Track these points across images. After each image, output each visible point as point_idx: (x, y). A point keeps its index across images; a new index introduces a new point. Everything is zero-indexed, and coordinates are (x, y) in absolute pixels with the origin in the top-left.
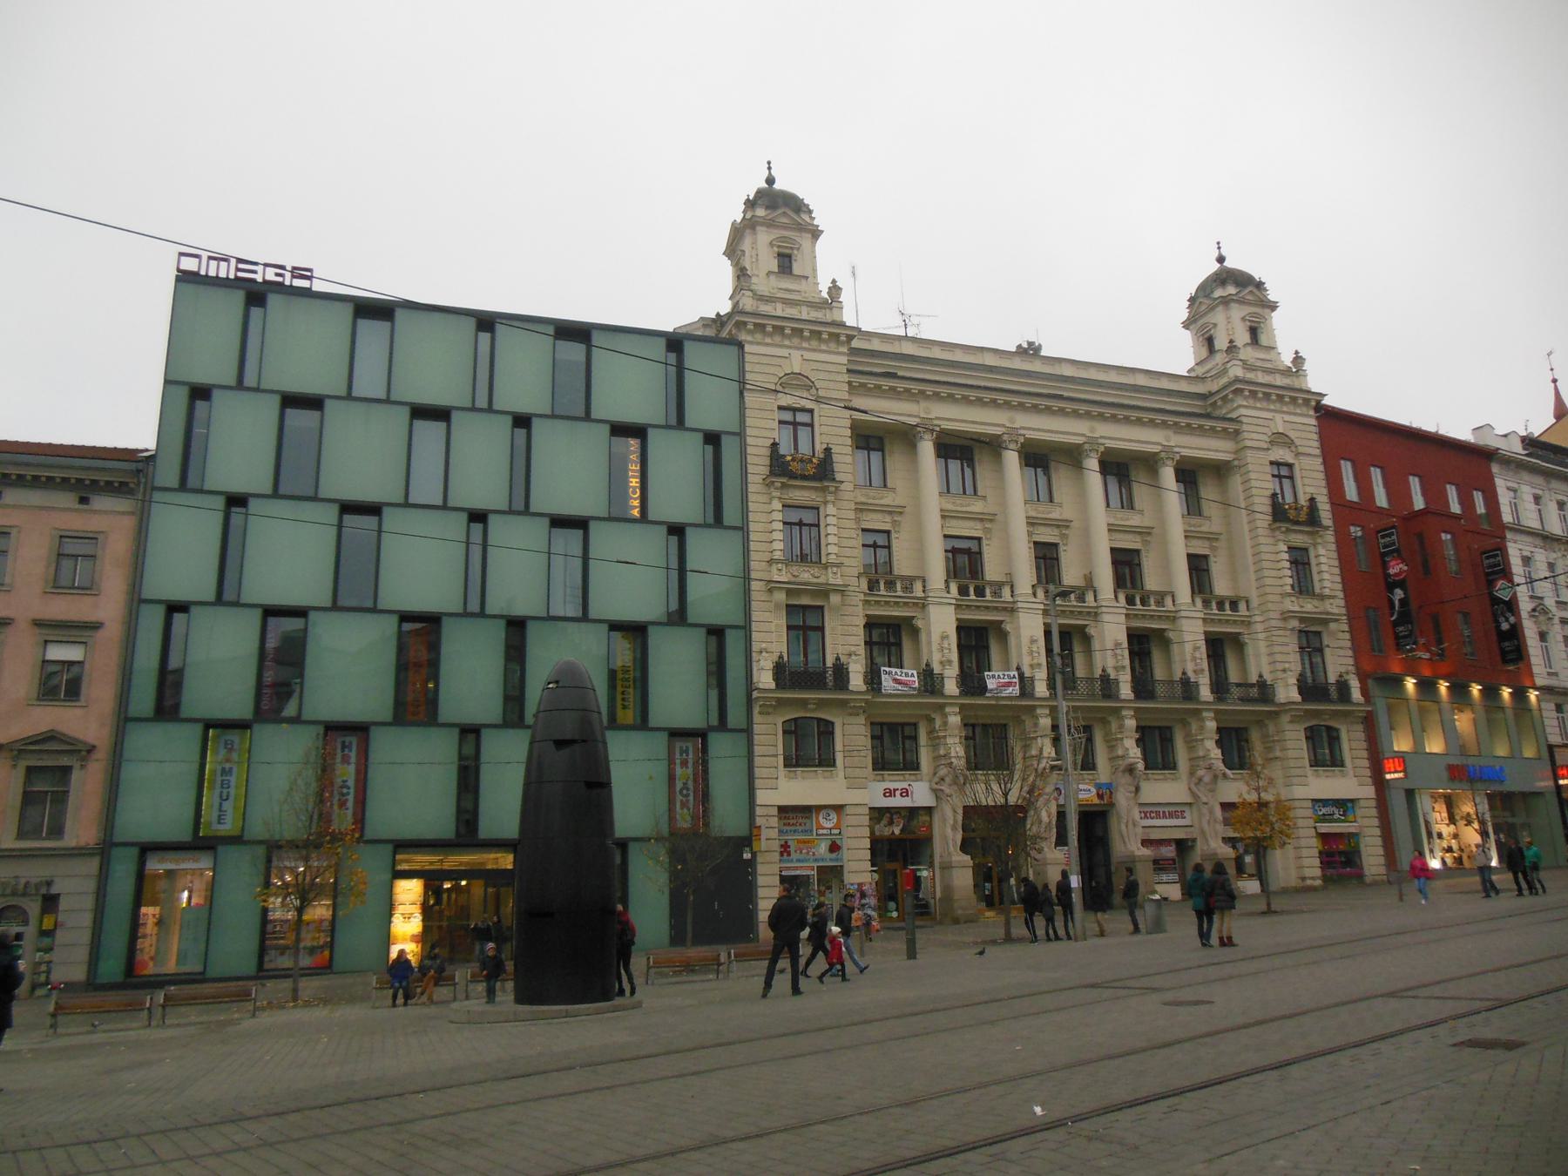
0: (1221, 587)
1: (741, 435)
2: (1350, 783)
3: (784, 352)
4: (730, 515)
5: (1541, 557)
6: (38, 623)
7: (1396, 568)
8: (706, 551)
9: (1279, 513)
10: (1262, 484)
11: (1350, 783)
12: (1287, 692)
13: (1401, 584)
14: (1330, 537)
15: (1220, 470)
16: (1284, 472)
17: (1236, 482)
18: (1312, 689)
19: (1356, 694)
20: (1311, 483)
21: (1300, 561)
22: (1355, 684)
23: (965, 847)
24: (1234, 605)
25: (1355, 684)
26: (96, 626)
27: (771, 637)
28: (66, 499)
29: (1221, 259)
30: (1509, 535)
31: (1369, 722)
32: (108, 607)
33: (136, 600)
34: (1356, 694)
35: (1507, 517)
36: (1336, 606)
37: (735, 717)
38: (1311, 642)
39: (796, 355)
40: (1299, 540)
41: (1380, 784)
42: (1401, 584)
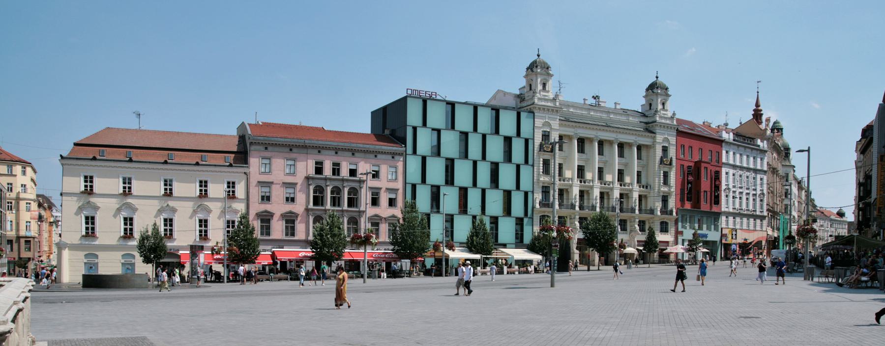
0: (643, 182)
1: (533, 139)
4: (530, 162)
5: (731, 171)
6: (387, 189)
7: (690, 178)
8: (525, 171)
10: (659, 153)
13: (691, 183)
14: (674, 169)
15: (647, 146)
16: (665, 150)
17: (652, 150)
19: (674, 214)
21: (666, 175)
22: (674, 211)
23: (577, 249)
24: (647, 187)
25: (674, 211)
27: (538, 197)
32: (399, 185)
33: (405, 183)
34: (674, 214)
35: (724, 160)
36: (673, 190)
38: (665, 200)
40: (666, 170)
42: (691, 183)
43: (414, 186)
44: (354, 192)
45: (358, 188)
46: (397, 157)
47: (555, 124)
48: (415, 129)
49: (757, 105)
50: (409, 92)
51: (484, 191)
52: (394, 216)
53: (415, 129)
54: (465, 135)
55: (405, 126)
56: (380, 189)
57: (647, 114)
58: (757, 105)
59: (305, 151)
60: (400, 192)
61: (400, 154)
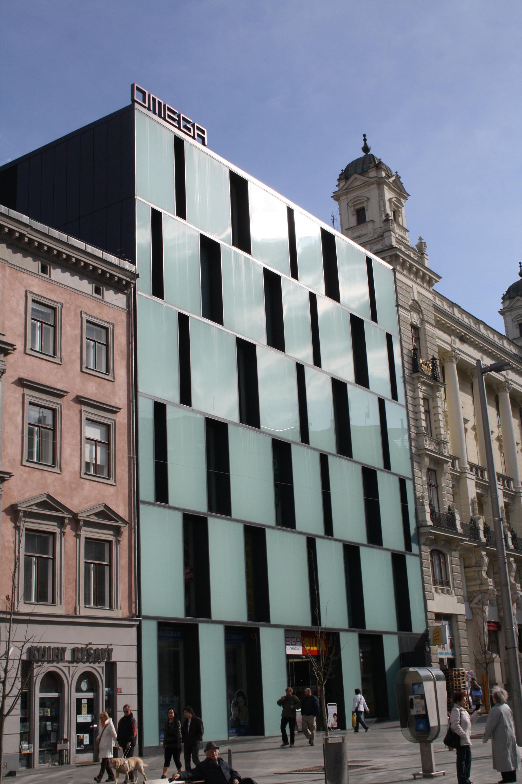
6: (79, 400)
26: (113, 410)
28: (86, 286)
39: (415, 286)
46: (110, 295)
52: (106, 513)
53: (157, 217)
56: (59, 394)
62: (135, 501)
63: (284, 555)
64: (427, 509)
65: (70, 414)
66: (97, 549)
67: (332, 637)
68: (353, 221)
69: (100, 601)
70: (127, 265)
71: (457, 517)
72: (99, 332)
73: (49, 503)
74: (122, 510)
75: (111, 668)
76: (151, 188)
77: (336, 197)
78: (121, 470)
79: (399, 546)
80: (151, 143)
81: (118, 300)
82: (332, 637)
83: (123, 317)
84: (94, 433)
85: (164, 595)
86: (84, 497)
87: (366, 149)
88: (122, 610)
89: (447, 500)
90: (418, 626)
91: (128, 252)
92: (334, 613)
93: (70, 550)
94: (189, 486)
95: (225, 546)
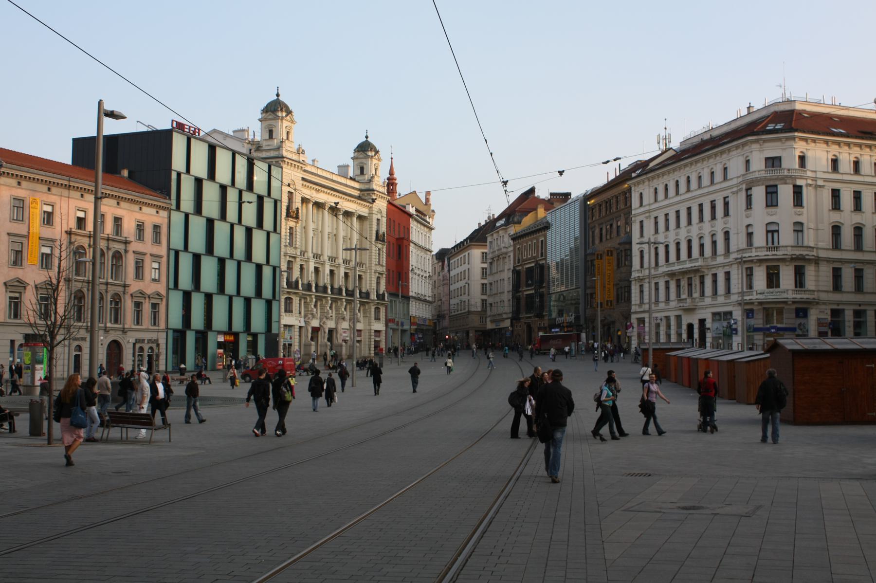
2: (380, 326)
3: (290, 172)
4: (278, 231)
6: (151, 255)
9: (377, 239)
11: (380, 326)
12: (373, 296)
17: (367, 223)
18: (378, 295)
20: (383, 229)
26: (161, 257)
29: (367, 137)
30: (412, 244)
31: (386, 308)
32: (162, 250)
33: (169, 249)
36: (384, 269)
37: (277, 298)
41: (387, 325)
43: (177, 253)
44: (118, 256)
45: (123, 252)
47: (299, 183)
48: (179, 175)
49: (391, 173)
50: (175, 125)
51: (239, 263)
52: (158, 294)
53: (179, 175)
54: (223, 188)
55: (169, 169)
56: (144, 254)
57: (357, 178)
58: (391, 173)
59: (65, 192)
60: (164, 260)
61: (164, 209)
62: (168, 289)
63: (220, 305)
64: (285, 280)
65: (148, 260)
66: (154, 306)
67: (236, 335)
68: (267, 136)
69: (155, 324)
70: (167, 201)
71: (300, 283)
72: (156, 228)
73: (142, 293)
74: (163, 292)
75: (158, 345)
76: (178, 162)
77: (260, 120)
78: (164, 279)
79: (270, 297)
80: (178, 143)
81: (164, 214)
82: (236, 335)
83: (166, 220)
84: (156, 265)
85: (176, 321)
86: (150, 289)
87: (278, 95)
88: (162, 325)
89: (296, 274)
90: (274, 330)
91: (169, 195)
92: (238, 325)
93: (147, 308)
94: (185, 281)
95: (198, 302)
